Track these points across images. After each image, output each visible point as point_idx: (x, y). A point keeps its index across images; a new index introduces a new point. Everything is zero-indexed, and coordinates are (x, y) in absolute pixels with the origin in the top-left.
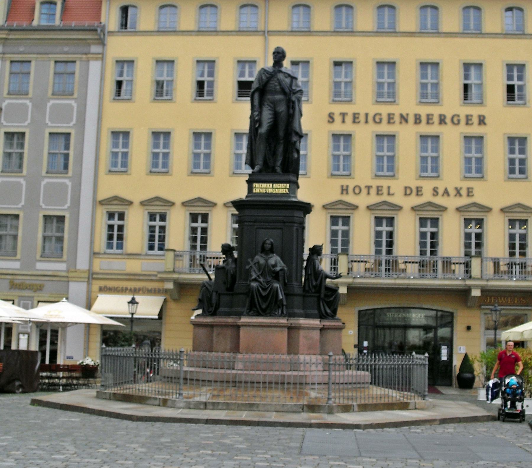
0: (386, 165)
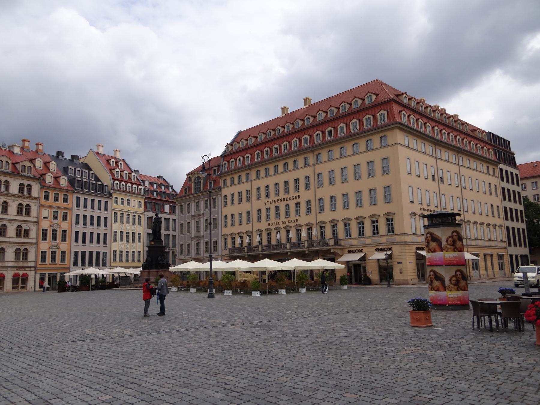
0: (278, 215)
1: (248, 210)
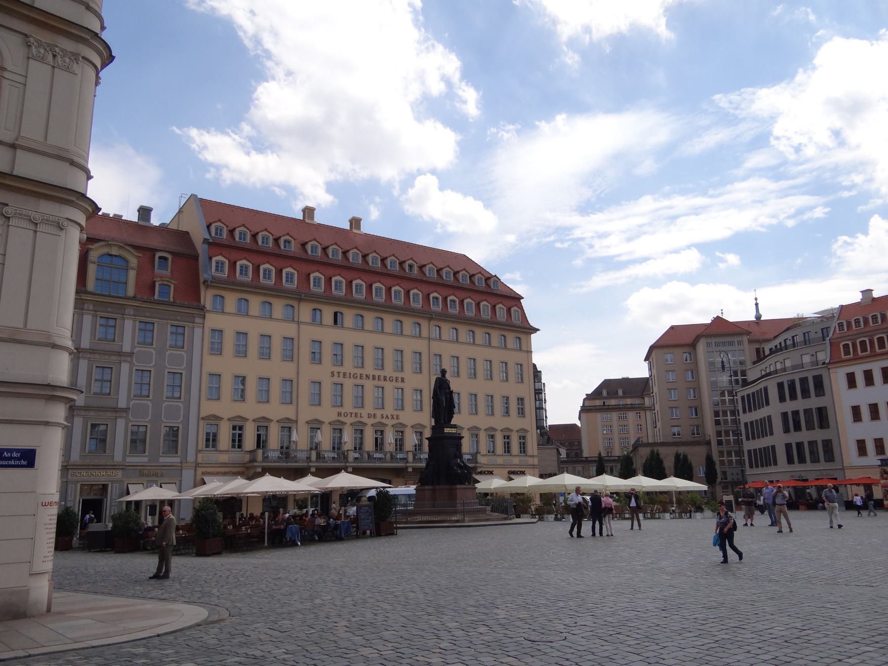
1: (287, 377)
